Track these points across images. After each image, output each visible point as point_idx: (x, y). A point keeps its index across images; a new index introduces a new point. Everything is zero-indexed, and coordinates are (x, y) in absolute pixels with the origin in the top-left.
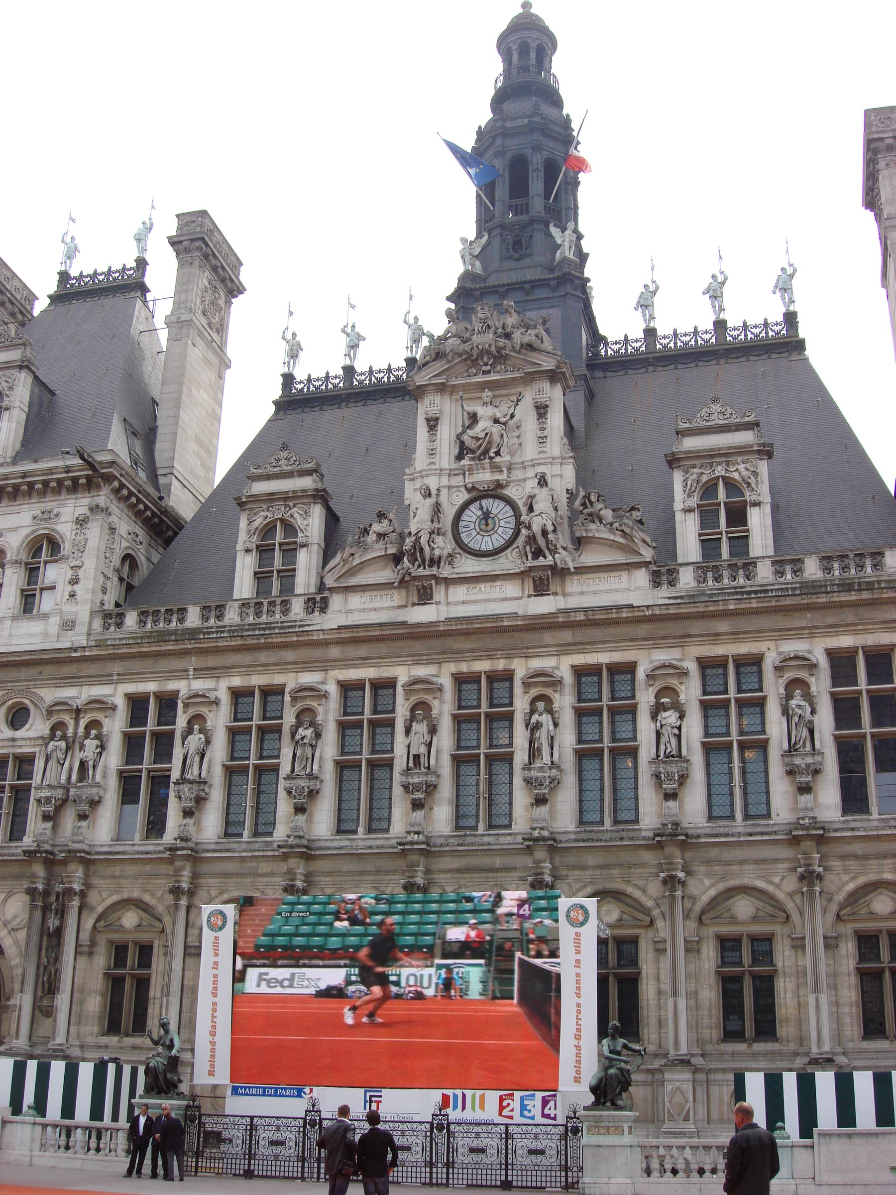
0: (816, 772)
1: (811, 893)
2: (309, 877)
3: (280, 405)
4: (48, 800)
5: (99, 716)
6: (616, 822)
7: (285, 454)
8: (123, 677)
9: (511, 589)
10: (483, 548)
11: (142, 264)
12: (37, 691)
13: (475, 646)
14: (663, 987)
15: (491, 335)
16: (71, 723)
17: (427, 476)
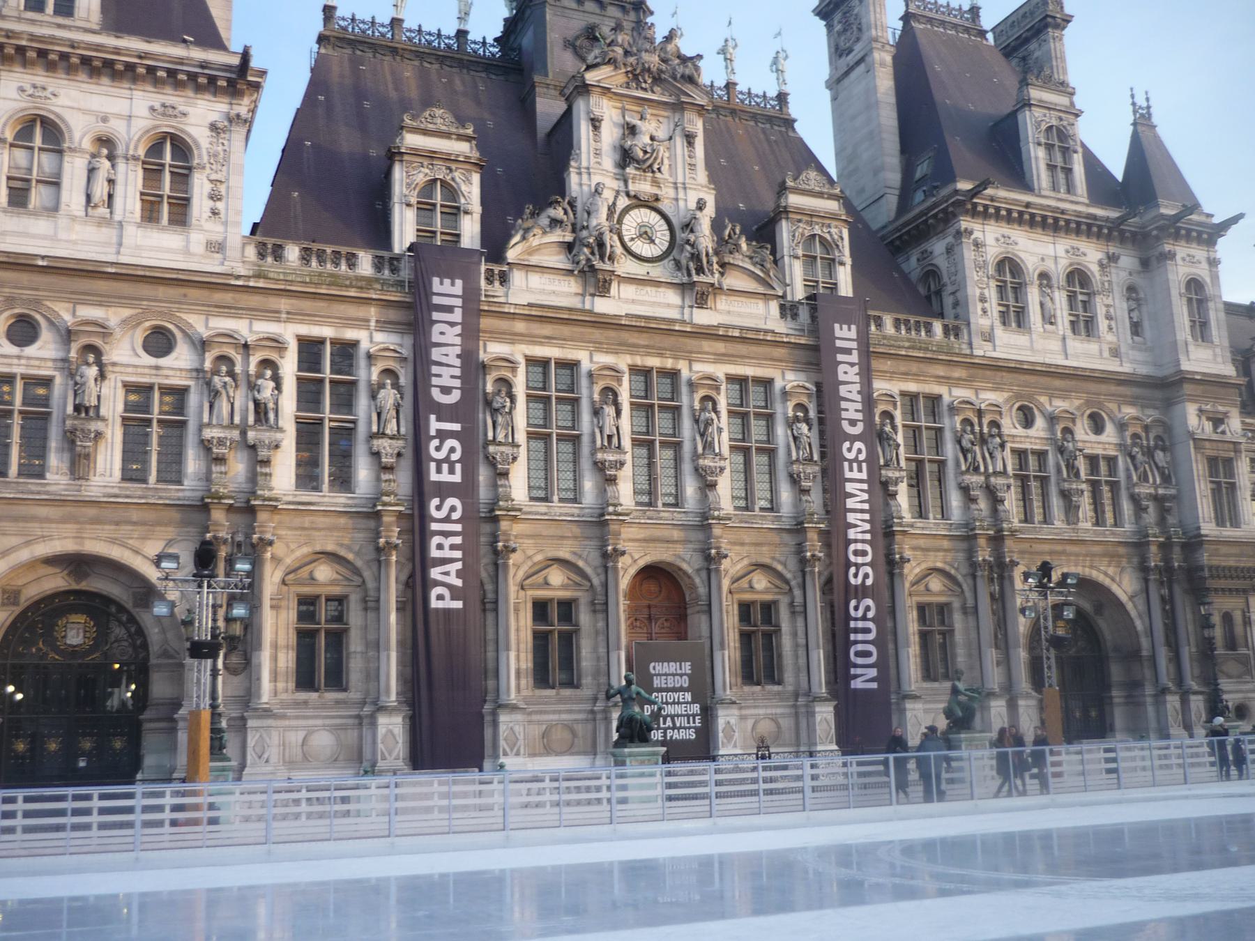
0: (896, 482)
3: (321, 39)
4: (221, 442)
5: (273, 356)
7: (439, 112)
8: (293, 316)
9: (672, 297)
10: (644, 254)
12: (184, 316)
13: (646, 343)
15: (657, 58)
16: (238, 359)
17: (595, 174)
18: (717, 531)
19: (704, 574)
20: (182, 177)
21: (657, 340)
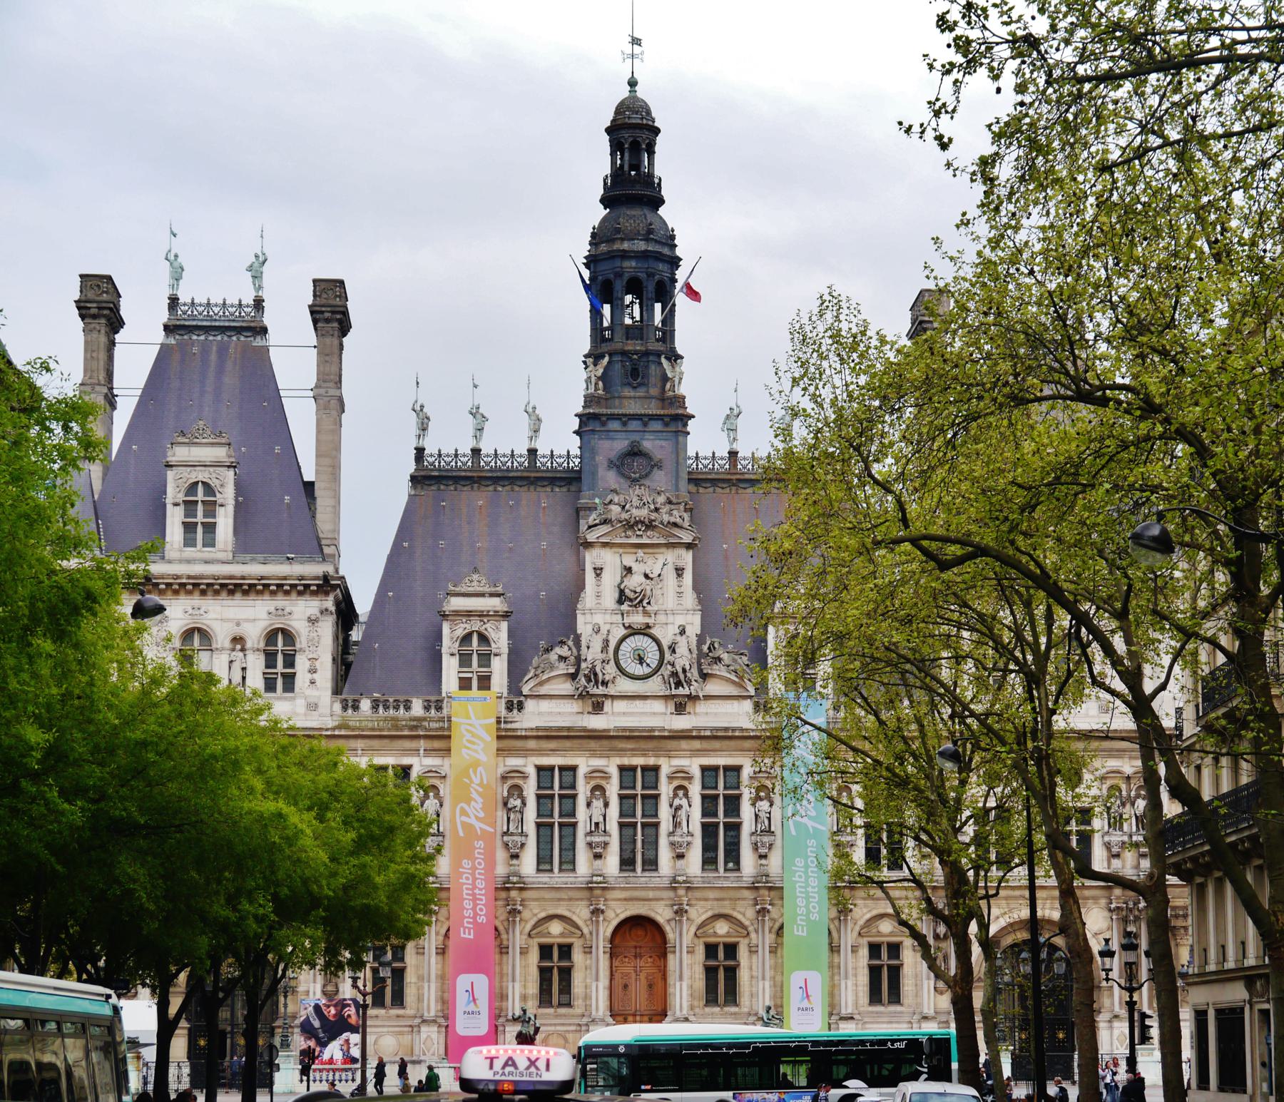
1: (846, 920)
2: (523, 900)
3: (414, 479)
6: (726, 870)
9: (658, 706)
10: (636, 673)
11: (259, 304)
14: (754, 974)
18: (681, 892)
19: (673, 923)
20: (290, 661)
21: (642, 744)
